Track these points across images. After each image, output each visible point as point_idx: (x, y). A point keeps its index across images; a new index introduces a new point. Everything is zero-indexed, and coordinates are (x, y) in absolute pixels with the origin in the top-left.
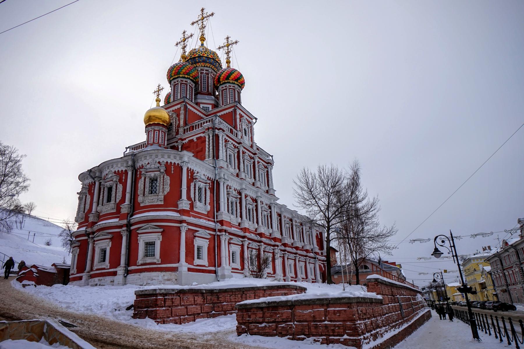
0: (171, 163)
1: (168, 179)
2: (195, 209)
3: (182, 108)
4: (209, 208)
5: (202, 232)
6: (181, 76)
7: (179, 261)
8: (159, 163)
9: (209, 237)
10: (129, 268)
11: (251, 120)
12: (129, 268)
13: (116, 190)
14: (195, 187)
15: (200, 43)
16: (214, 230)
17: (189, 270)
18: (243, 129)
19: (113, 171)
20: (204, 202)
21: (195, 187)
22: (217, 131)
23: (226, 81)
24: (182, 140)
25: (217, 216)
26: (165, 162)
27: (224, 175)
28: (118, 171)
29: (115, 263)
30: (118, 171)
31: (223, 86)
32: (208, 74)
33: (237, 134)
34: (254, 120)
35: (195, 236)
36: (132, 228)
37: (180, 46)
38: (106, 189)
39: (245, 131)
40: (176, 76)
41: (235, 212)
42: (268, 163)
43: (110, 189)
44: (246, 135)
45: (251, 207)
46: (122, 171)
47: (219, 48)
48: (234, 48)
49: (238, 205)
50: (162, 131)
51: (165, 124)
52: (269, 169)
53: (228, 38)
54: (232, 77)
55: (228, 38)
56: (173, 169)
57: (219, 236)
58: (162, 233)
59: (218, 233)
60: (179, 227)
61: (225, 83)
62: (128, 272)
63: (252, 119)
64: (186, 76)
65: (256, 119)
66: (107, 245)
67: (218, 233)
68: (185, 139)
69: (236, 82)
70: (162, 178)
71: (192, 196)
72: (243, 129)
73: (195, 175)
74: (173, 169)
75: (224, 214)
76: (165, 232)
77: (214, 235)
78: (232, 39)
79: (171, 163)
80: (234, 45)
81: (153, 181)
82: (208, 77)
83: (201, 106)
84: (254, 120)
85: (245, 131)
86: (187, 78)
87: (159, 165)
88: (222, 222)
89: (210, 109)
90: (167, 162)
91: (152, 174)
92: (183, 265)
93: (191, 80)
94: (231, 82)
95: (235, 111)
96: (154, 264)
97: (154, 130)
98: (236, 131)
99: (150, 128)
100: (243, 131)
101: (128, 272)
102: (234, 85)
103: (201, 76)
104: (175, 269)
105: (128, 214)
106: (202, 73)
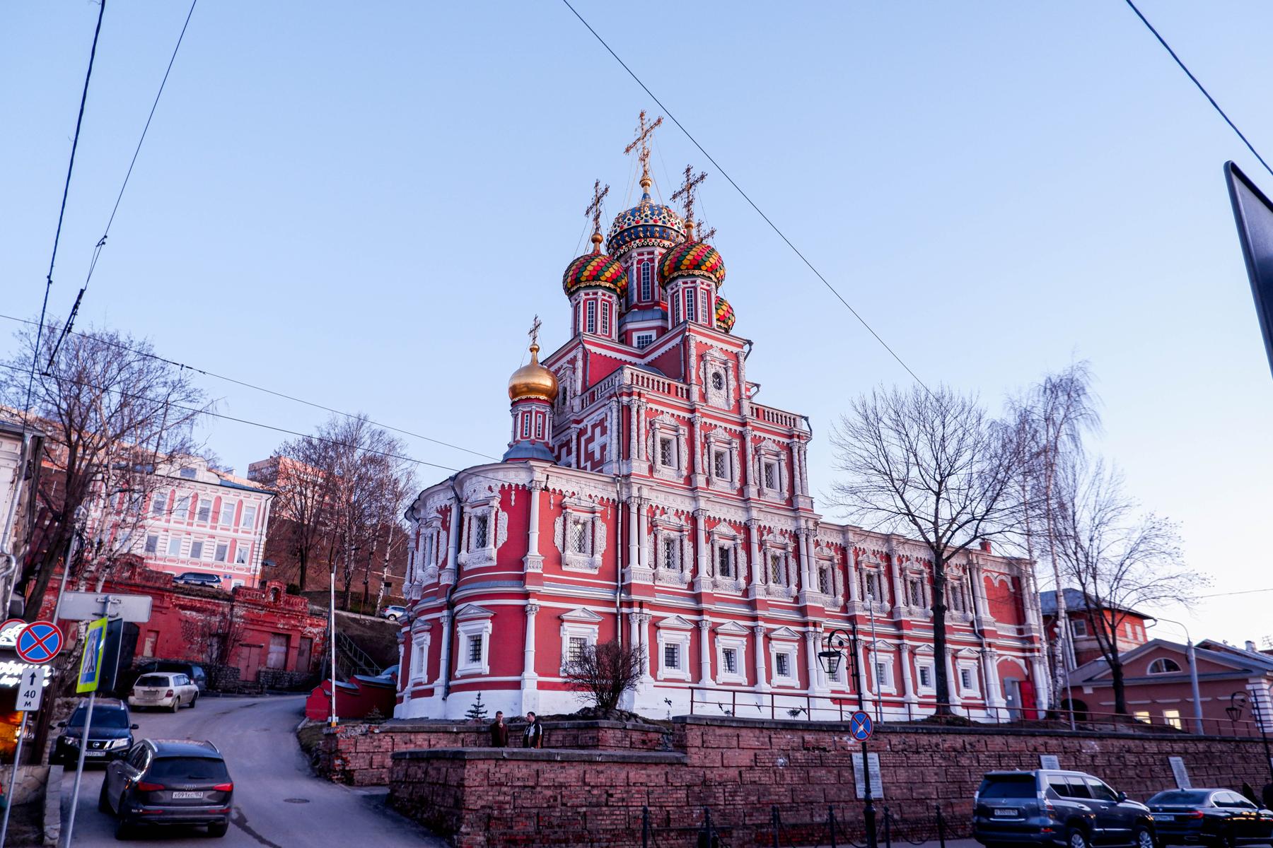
0: (510, 485)
1: (504, 517)
2: (564, 568)
3: (580, 356)
4: (598, 558)
5: (578, 610)
7: (521, 669)
8: (490, 488)
9: (598, 619)
10: (451, 683)
11: (735, 350)
12: (451, 683)
14: (565, 525)
15: (641, 191)
16: (611, 603)
17: (541, 686)
18: (710, 375)
20: (589, 551)
21: (565, 525)
22: (625, 399)
23: (675, 274)
24: (578, 422)
25: (623, 575)
27: (639, 489)
29: (433, 673)
31: (673, 285)
32: (652, 260)
33: (688, 391)
34: (746, 348)
35: (563, 621)
36: (456, 609)
37: (592, 216)
39: (716, 375)
41: (678, 562)
42: (791, 437)
44: (719, 387)
45: (728, 544)
47: (675, 197)
48: (699, 191)
49: (688, 546)
50: (537, 412)
51: (543, 397)
52: (795, 450)
53: (688, 170)
54: (686, 262)
55: (688, 170)
56: (513, 497)
57: (626, 618)
58: (492, 618)
59: (625, 610)
60: (524, 607)
61: (675, 279)
62: (449, 690)
63: (742, 347)
64: (593, 284)
65: (750, 343)
66: (427, 638)
67: (625, 610)
68: (581, 421)
69: (696, 272)
70: (493, 517)
71: (558, 542)
72: (710, 375)
73: (566, 499)
74: (513, 497)
75: (639, 571)
76: (498, 615)
77: (615, 615)
78: (696, 173)
79: (510, 485)
80: (699, 184)
81: (483, 521)
82: (653, 268)
83: (635, 335)
84: (746, 348)
85: (716, 375)
87: (489, 494)
88: (628, 589)
89: (654, 338)
91: (479, 511)
92: (530, 676)
95: (685, 341)
96: (480, 675)
97: (524, 413)
98: (685, 387)
99: (521, 408)
100: (710, 380)
101: (449, 690)
103: (638, 269)
104: (517, 686)
105: (448, 586)
106: (639, 262)
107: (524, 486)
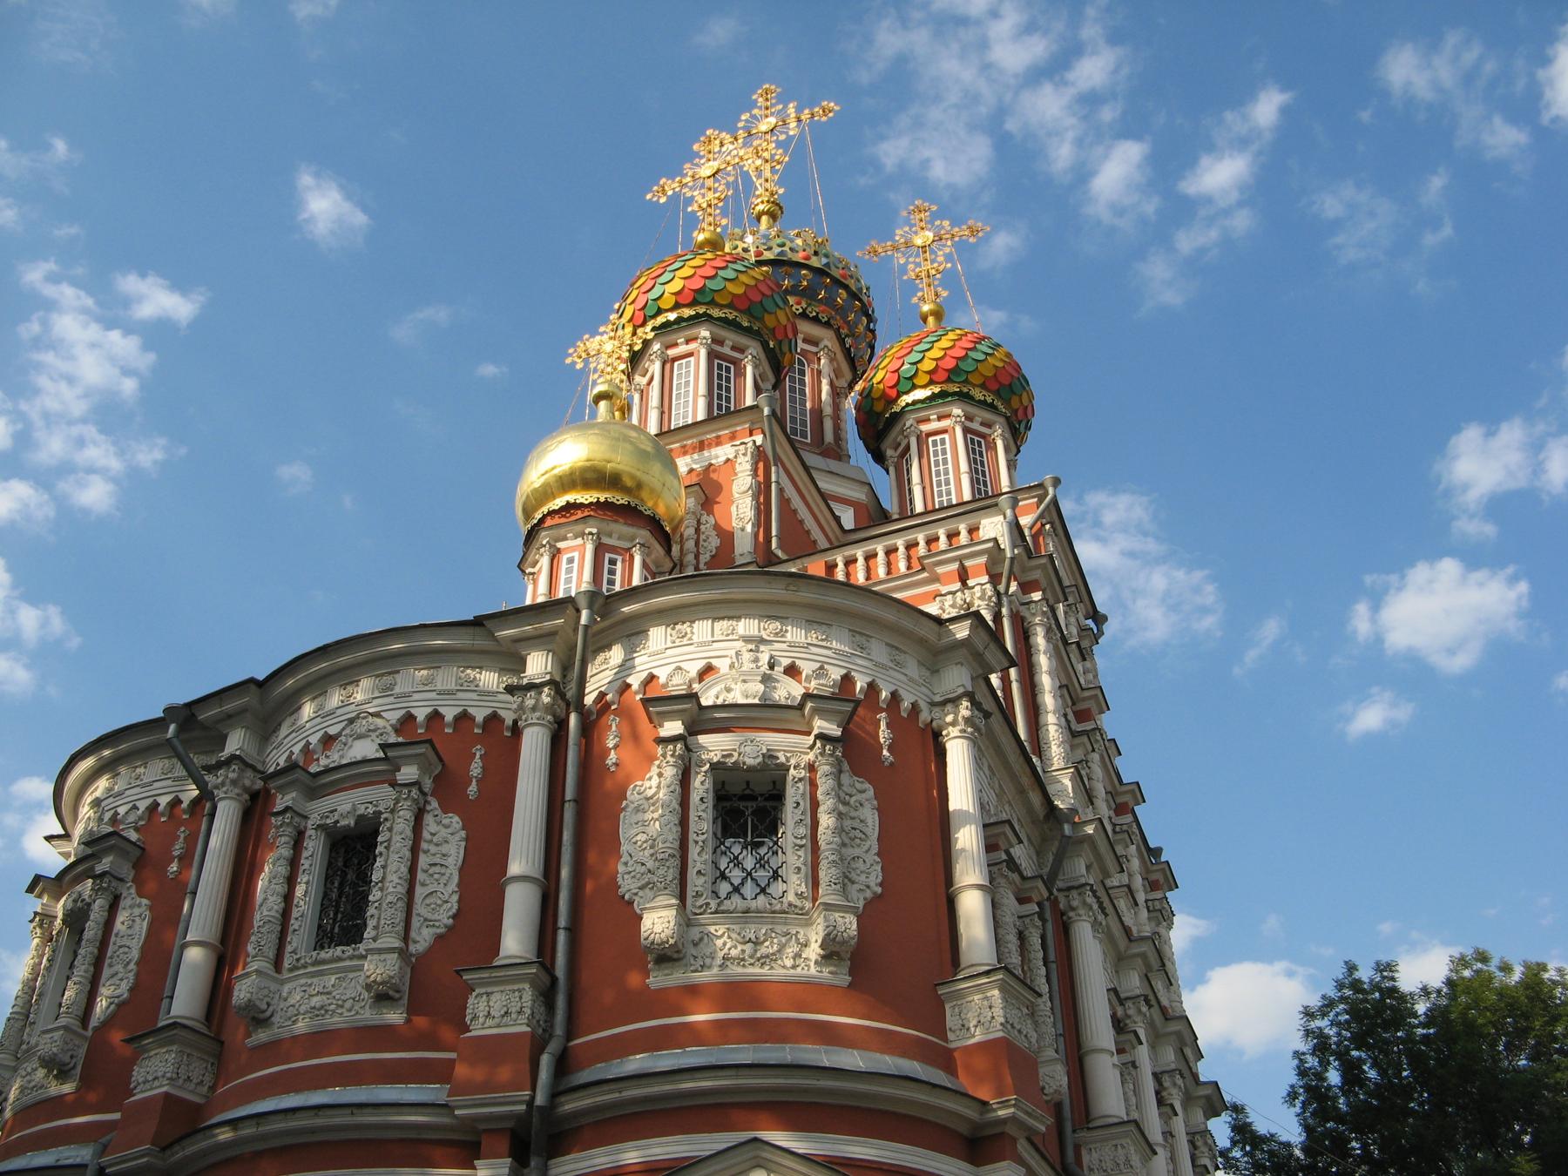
3: (744, 465)
6: (716, 313)
13: (415, 850)
19: (394, 716)
26: (836, 674)
28: (435, 716)
30: (435, 716)
38: (315, 847)
40: (687, 312)
43: (353, 849)
46: (464, 718)
79: (872, 688)
86: (748, 331)
90: (847, 679)
93: (765, 345)
94: (978, 394)
102: (988, 416)
107: (915, 708)
